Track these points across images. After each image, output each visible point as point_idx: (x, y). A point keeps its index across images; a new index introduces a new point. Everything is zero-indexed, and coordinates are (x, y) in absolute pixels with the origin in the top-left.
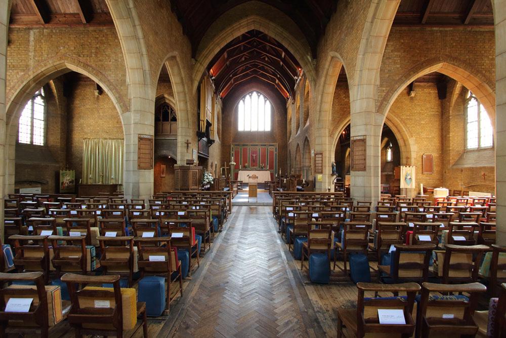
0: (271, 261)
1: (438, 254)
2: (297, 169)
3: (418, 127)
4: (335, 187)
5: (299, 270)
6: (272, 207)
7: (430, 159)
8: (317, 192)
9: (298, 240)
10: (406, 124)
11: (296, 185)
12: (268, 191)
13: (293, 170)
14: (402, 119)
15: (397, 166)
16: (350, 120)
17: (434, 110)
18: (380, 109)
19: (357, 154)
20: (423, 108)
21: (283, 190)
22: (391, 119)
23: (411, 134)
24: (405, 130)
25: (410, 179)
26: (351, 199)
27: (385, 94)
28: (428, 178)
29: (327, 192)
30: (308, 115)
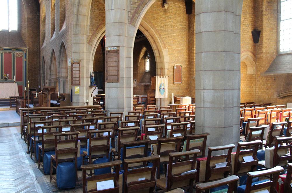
0: (17, 181)
1: (154, 146)
2: (53, 81)
3: (170, 39)
4: (94, 100)
5: (47, 183)
6: (19, 128)
7: (179, 69)
8: (74, 106)
9: (47, 155)
10: (160, 35)
11: (50, 99)
12: (16, 108)
13: (47, 81)
14: (157, 30)
15: (153, 77)
16: (105, 31)
17: (183, 24)
18: (132, 20)
19: (111, 65)
20: (174, 21)
21: (35, 106)
22: (148, 29)
23: (165, 45)
24: (159, 41)
25: (164, 88)
26: (106, 111)
27: (137, 6)
28: (178, 87)
29: (85, 105)
30: (65, 17)
